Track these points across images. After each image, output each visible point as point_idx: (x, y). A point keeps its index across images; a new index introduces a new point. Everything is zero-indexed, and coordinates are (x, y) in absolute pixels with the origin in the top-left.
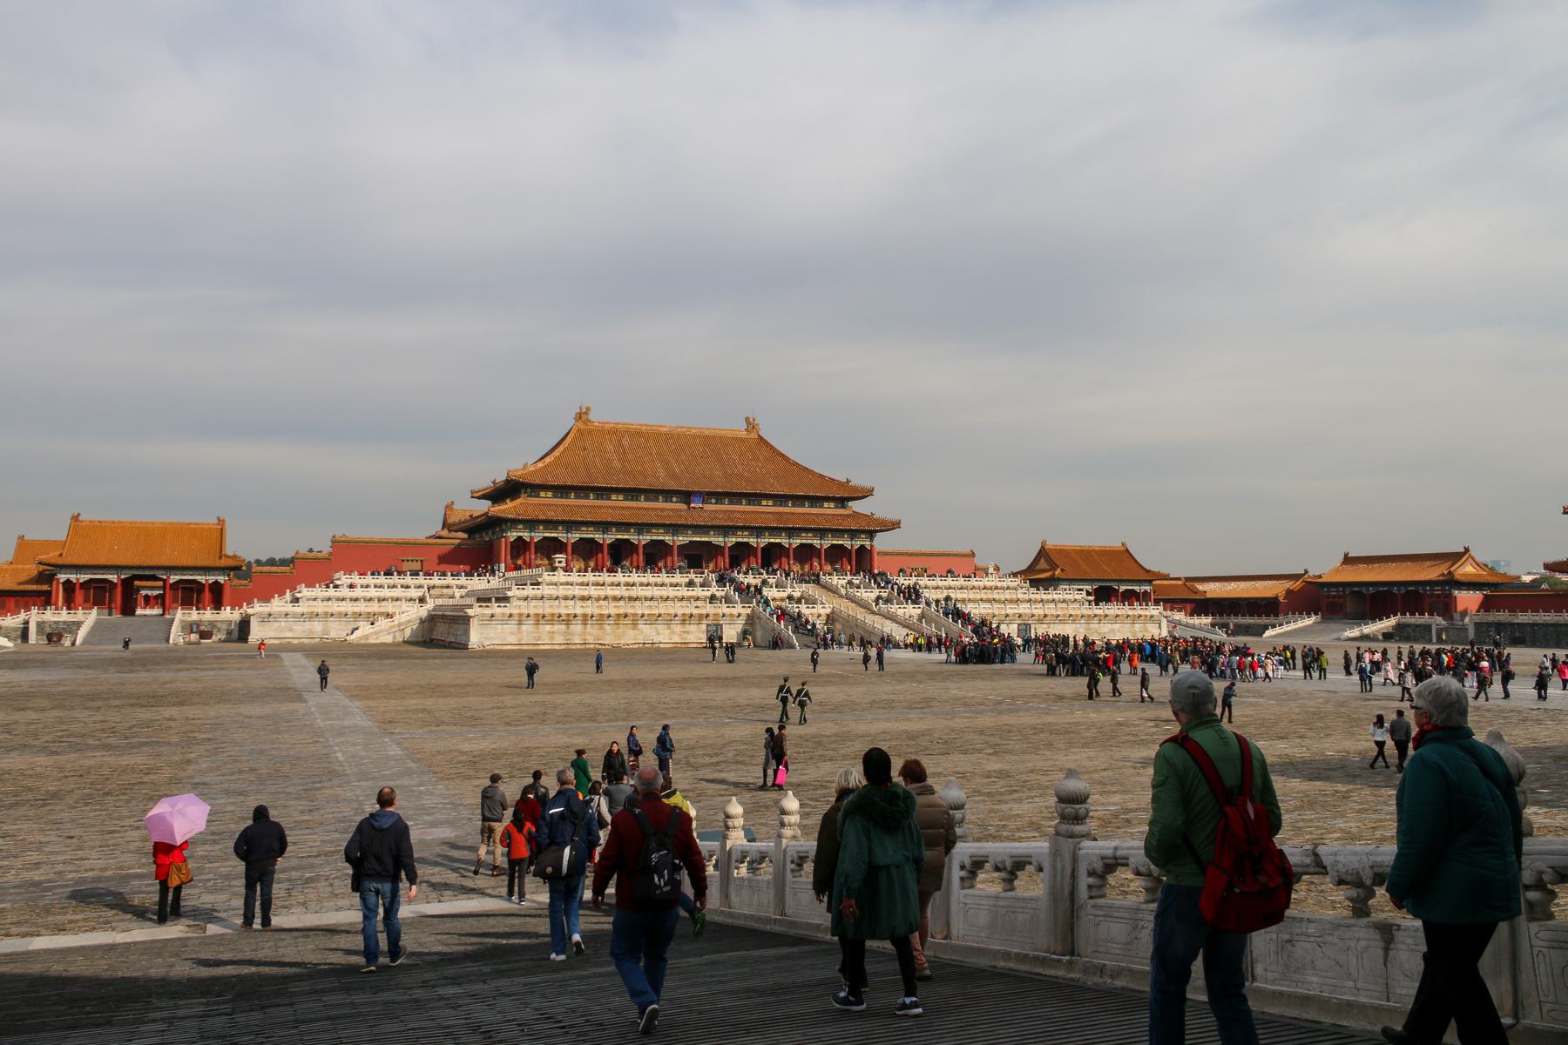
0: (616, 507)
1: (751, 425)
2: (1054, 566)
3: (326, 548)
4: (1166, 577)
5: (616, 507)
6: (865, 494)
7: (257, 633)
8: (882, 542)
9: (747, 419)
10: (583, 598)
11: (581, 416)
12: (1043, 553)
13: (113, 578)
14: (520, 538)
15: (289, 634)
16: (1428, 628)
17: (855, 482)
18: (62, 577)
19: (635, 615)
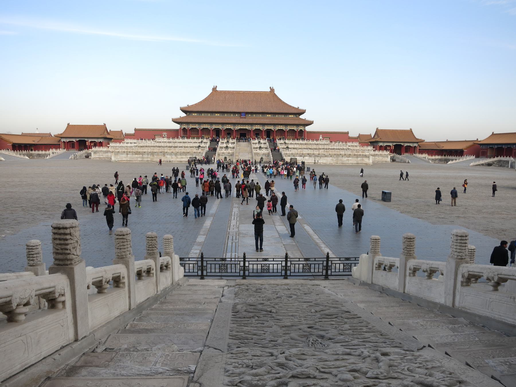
0: (217, 118)
1: (272, 90)
2: (378, 137)
3: (133, 132)
4: (423, 141)
5: (217, 118)
6: (303, 112)
7: (93, 156)
8: (308, 129)
9: (270, 88)
10: (159, 147)
11: (214, 89)
12: (376, 133)
13: (74, 140)
14: (184, 128)
15: (102, 157)
16: (508, 162)
17: (301, 108)
18: (63, 140)
19: (164, 152)
